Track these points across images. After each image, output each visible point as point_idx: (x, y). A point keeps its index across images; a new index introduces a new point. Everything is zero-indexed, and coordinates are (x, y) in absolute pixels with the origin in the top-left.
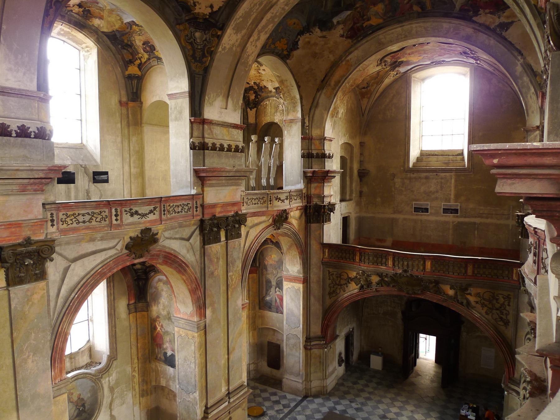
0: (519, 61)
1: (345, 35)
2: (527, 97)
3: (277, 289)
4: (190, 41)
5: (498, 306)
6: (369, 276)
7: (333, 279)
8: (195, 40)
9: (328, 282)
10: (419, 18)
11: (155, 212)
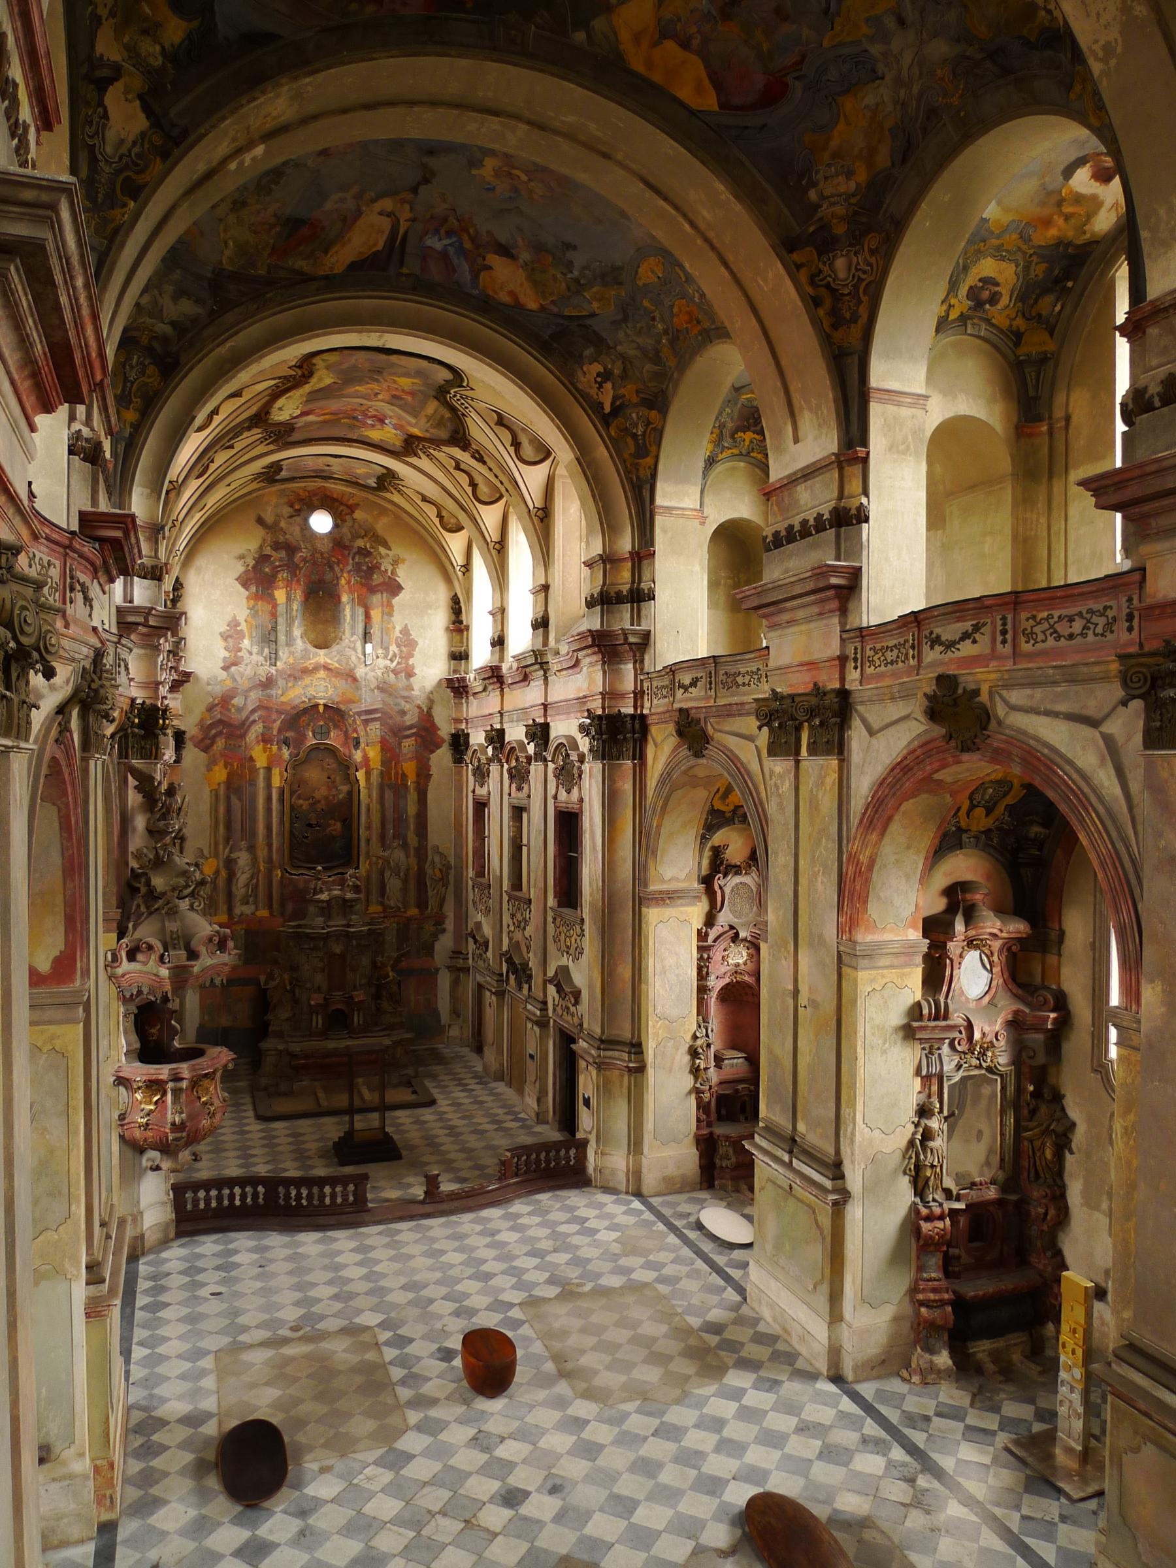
11: (977, 636)
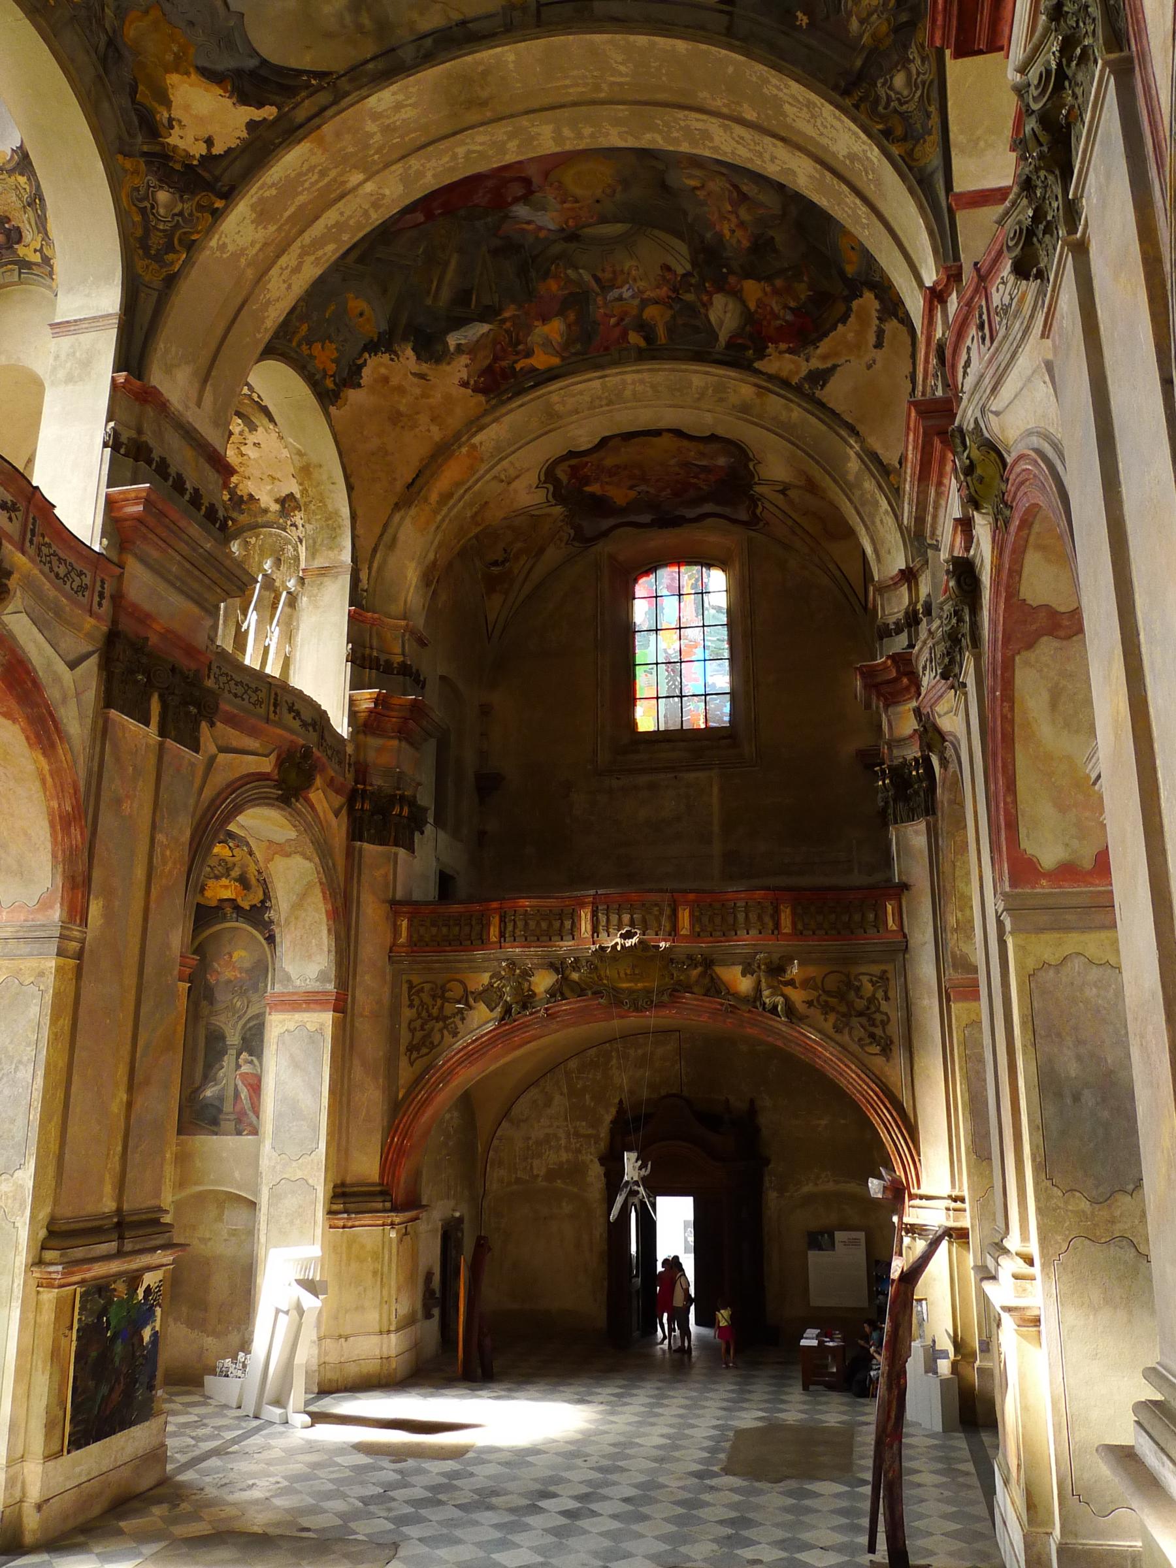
0: (852, 447)
1: (472, 382)
2: (873, 523)
3: (245, 1055)
4: (142, 205)
5: (860, 1004)
6: (526, 974)
7: (422, 1003)
8: (153, 207)
9: (408, 1013)
10: (641, 360)
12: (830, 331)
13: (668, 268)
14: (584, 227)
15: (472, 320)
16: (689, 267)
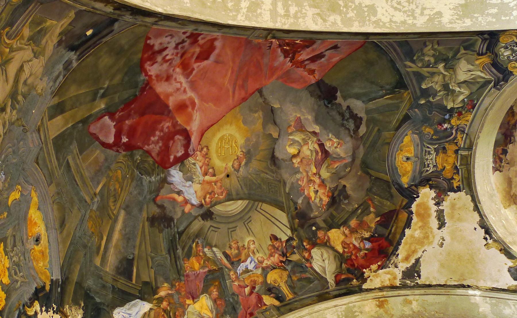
12: (401, 238)
13: (274, 238)
14: (216, 204)
15: (135, 297)
16: (289, 233)
